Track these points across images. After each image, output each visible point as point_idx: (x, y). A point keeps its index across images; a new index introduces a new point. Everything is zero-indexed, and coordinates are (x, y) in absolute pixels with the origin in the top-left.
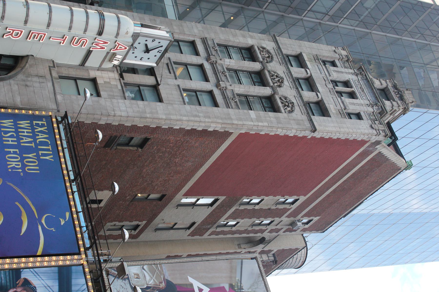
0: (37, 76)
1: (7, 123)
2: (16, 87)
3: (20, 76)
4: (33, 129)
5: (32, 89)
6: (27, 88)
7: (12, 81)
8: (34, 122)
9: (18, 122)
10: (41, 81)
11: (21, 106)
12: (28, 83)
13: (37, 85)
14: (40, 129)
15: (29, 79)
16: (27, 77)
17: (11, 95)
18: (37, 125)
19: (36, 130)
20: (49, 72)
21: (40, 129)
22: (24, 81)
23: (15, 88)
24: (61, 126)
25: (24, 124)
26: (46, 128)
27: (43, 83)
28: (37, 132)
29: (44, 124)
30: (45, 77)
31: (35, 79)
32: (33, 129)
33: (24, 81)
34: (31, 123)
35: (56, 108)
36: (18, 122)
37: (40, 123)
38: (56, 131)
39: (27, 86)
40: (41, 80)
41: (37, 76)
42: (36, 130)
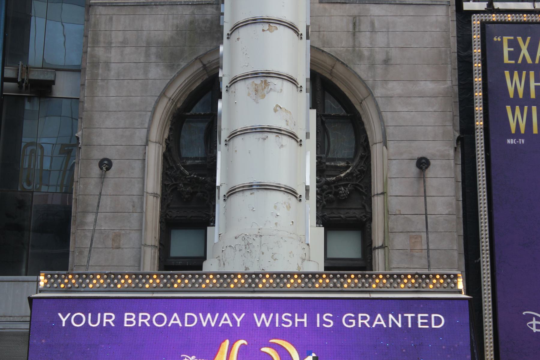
0: (354, 34)
1: (516, 119)
2: (391, 85)
3: (361, 69)
4: (523, 67)
5: (394, 53)
6: (392, 62)
7: (378, 92)
8: (506, 60)
9: (511, 95)
10: (369, 29)
11: (449, 83)
12: (380, 57)
13: (381, 39)
14: (524, 51)
15: (366, 53)
16: (360, 56)
17: (420, 99)
18: (514, 55)
19: (529, 61)
20: (338, 5)
21: (524, 51)
22: (372, 66)
23: (395, 88)
24: (497, 5)
25: (514, 84)
26: (520, 39)
27: (372, 24)
28: (533, 57)
29: (509, 40)
30: (355, 17)
31: (364, 39)
32: (523, 67)
33: (372, 66)
34: (512, 68)
35: (444, 8)
36: (511, 95)
37: (506, 50)
38: (509, 18)
39: (387, 62)
40: (365, 26)
41: (354, 34)
42: (529, 61)
